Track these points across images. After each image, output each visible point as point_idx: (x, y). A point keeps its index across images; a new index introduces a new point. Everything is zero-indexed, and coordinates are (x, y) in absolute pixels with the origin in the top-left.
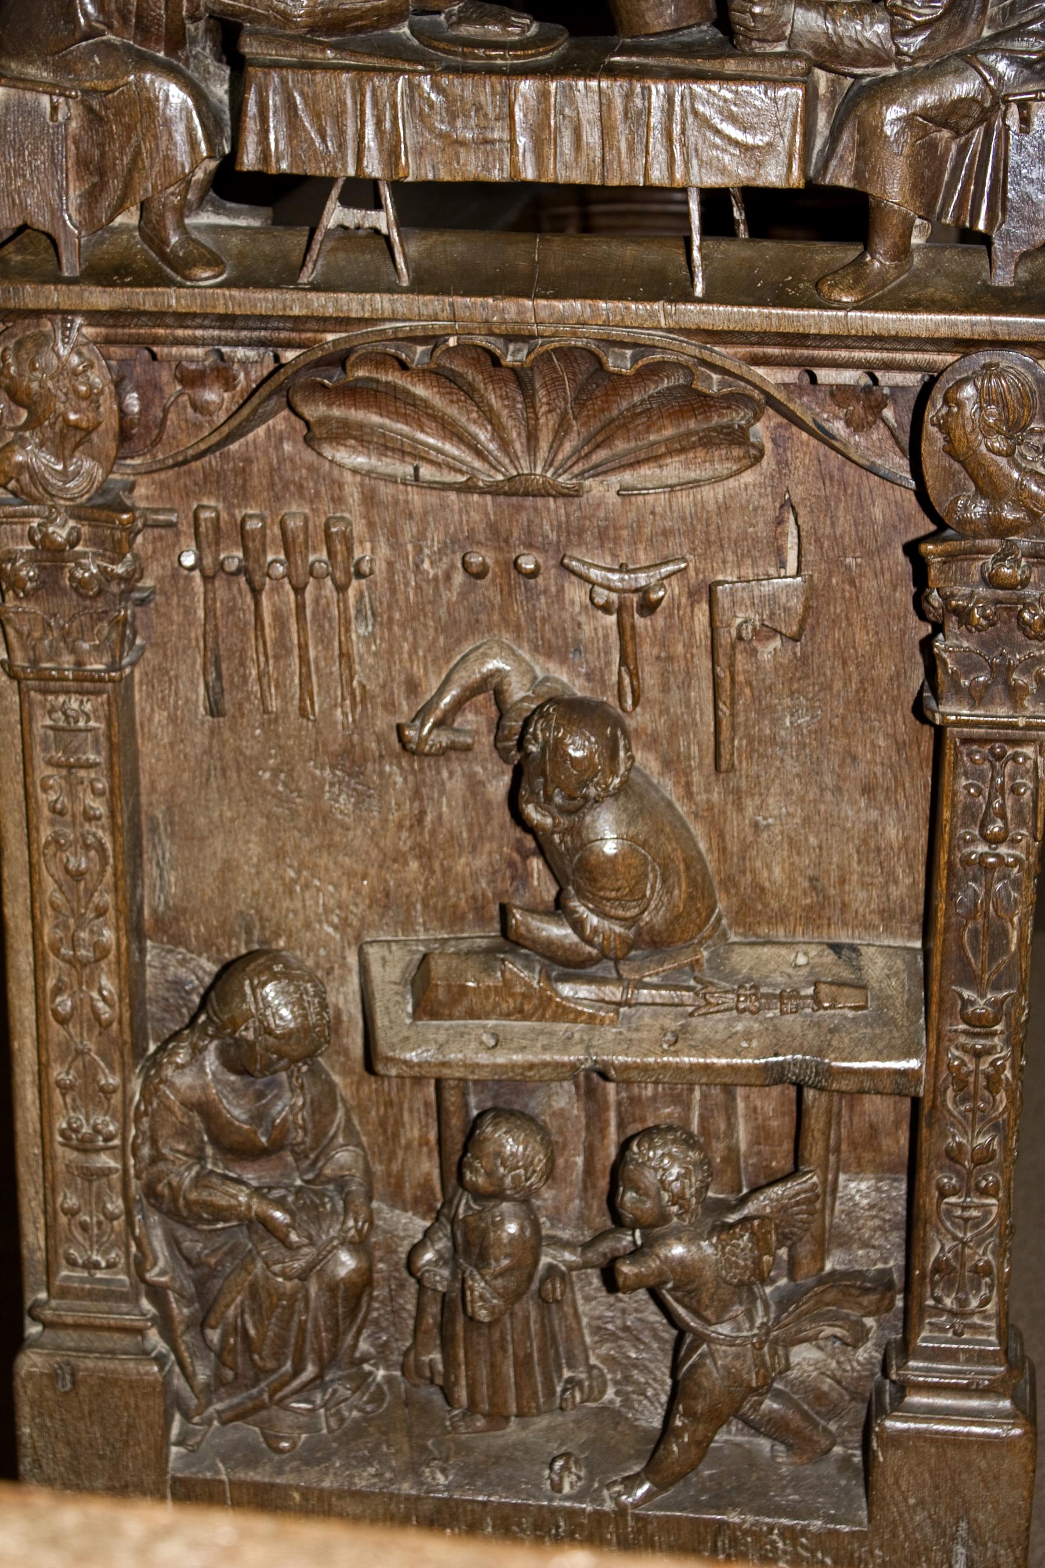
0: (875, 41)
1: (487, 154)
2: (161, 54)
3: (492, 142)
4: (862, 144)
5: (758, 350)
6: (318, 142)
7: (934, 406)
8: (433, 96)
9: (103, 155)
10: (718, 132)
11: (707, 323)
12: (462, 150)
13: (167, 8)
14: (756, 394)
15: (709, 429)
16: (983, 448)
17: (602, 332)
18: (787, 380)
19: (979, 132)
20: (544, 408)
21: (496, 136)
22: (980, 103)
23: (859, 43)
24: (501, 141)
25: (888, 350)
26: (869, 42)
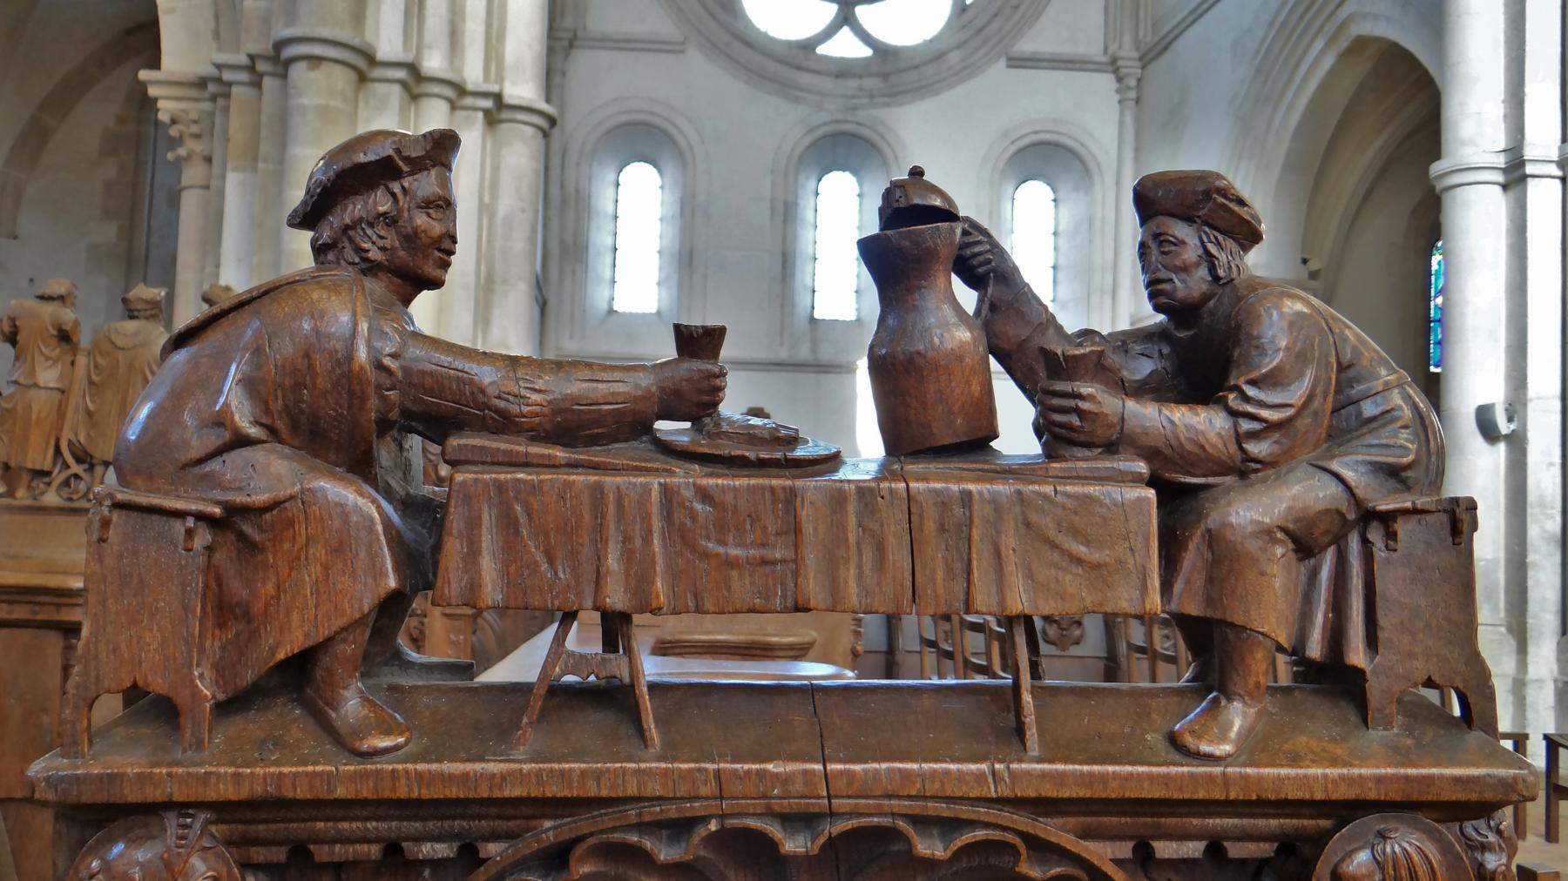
0: (1220, 445)
3: (773, 562)
5: (1092, 820)
6: (544, 567)
8: (699, 507)
10: (1054, 546)
11: (1049, 791)
12: (735, 573)
17: (916, 807)
18: (1120, 855)
21: (778, 555)
23: (1202, 447)
24: (783, 561)
25: (1286, 816)
26: (1215, 446)
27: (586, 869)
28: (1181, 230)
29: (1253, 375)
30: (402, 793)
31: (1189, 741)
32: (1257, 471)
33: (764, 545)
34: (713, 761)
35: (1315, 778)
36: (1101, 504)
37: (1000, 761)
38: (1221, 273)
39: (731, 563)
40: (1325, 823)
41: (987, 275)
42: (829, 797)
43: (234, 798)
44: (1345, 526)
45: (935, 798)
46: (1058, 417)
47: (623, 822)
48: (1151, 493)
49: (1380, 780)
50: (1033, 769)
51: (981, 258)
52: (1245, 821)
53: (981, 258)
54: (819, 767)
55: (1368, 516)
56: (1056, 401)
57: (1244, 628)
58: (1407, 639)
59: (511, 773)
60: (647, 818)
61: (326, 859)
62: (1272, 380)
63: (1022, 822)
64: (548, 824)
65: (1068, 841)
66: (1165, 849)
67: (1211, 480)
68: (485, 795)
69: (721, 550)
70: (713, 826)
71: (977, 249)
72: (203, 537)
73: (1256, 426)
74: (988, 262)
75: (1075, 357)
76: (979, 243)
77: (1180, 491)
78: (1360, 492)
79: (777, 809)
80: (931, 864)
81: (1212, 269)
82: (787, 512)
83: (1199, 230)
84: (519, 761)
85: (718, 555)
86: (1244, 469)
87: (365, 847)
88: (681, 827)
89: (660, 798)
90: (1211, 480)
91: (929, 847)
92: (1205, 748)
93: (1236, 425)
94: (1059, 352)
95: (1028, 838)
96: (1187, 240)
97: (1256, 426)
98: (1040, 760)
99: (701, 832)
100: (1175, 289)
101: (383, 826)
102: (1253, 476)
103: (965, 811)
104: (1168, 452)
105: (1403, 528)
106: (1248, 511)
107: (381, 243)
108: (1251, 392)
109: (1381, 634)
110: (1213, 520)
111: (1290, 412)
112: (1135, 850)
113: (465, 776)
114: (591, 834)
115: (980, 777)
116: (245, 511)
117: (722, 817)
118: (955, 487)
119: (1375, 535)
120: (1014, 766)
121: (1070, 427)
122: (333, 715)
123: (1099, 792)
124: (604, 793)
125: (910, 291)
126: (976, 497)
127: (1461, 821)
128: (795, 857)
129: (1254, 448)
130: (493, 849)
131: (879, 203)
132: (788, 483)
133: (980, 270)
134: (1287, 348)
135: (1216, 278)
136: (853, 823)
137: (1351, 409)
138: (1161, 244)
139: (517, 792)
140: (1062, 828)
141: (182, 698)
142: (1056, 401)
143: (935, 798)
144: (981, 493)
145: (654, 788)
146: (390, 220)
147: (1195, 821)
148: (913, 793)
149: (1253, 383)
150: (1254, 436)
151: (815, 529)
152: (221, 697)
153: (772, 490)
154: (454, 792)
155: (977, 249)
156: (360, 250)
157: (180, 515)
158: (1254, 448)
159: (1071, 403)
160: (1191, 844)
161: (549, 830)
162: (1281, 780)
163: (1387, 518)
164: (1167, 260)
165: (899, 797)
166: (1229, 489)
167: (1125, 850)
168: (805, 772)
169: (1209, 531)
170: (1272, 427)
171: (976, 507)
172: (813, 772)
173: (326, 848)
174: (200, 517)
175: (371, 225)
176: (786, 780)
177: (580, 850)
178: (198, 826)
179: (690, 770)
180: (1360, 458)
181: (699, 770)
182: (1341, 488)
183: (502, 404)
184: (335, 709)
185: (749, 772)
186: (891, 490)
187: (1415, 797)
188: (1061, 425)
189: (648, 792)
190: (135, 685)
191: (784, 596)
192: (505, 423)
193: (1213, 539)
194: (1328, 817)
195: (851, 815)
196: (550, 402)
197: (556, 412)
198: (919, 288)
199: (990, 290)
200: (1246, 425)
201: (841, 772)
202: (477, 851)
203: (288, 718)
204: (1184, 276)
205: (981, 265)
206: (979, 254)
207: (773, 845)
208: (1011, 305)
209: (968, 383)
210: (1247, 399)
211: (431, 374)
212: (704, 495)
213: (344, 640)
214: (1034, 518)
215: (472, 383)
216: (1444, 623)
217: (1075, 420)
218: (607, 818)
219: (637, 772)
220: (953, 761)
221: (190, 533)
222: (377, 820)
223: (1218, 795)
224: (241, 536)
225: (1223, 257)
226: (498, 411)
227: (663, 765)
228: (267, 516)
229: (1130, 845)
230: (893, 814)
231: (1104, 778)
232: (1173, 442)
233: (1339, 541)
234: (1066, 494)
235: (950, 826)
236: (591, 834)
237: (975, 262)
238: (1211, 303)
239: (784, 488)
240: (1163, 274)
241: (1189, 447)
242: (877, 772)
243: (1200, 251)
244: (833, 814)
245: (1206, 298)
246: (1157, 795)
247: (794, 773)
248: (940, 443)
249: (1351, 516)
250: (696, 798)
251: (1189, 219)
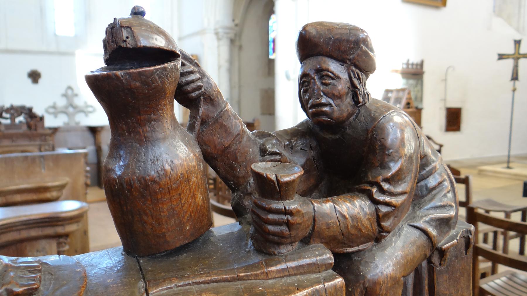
23: (360, 230)
28: (334, 67)
41: (198, 98)
51: (194, 85)
53: (194, 85)
56: (271, 217)
67: (361, 247)
74: (200, 88)
76: (191, 72)
83: (348, 69)
90: (361, 247)
93: (377, 210)
96: (341, 75)
100: (333, 111)
104: (340, 237)
108: (386, 186)
125: (141, 124)
131: (103, 36)
133: (193, 95)
137: (422, 183)
138: (321, 78)
149: (387, 180)
164: (328, 89)
169: (366, 288)
198: (149, 121)
199: (201, 110)
200: (384, 209)
204: (338, 102)
205: (194, 90)
206: (192, 82)
208: (216, 121)
209: (194, 197)
210: (382, 191)
232: (344, 231)
237: (189, 88)
241: (353, 231)
243: (349, 84)
248: (173, 247)
251: (342, 61)
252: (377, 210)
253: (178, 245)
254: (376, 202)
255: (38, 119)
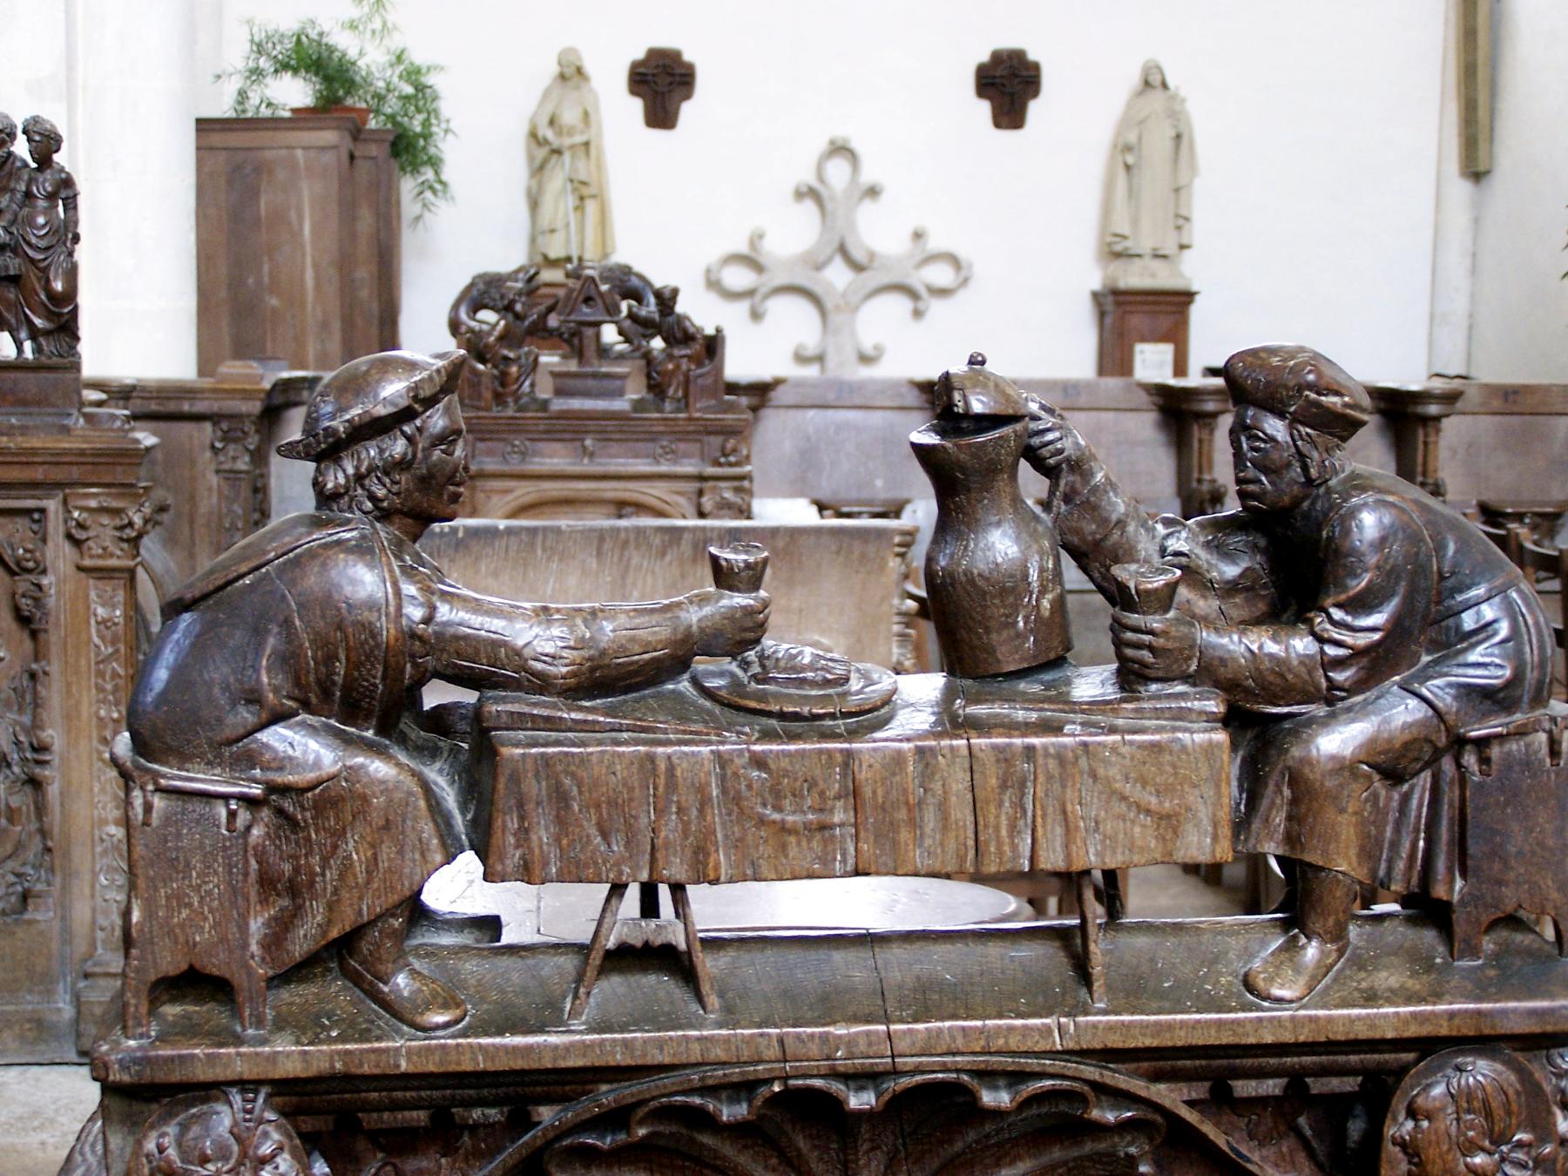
1: (825, 842)
2: (370, 734)
3: (831, 827)
4: (1294, 801)
7: (1395, 1119)
9: (297, 870)
10: (1124, 798)
11: (1115, 1041)
12: (792, 839)
13: (384, 678)
14: (1159, 1119)
15: (1080, 1158)
16: (1462, 1167)
18: (1194, 1095)
19: (1425, 778)
20: (866, 1146)
21: (836, 819)
22: (1428, 740)
23: (1283, 676)
24: (842, 825)
27: (642, 1132)
29: (1343, 597)
30: (467, 1066)
31: (1260, 983)
32: (1343, 699)
33: (821, 810)
34: (776, 1027)
35: (1386, 1016)
36: (1171, 753)
37: (1067, 1015)
38: (1313, 472)
39: (783, 829)
40: (1411, 1056)
42: (893, 1057)
43: (303, 1075)
44: (1437, 754)
45: (999, 1053)
46: (1129, 652)
47: (686, 1086)
48: (1221, 736)
49: (1452, 1015)
50: (1104, 1022)
52: (1324, 1058)
54: (884, 1027)
55: (1459, 743)
56: (1129, 635)
57: (1322, 869)
58: (1497, 866)
59: (572, 1044)
60: (710, 1082)
61: (373, 1126)
62: (1362, 604)
63: (1091, 1072)
64: (604, 1088)
65: (1138, 1086)
66: (1245, 1088)
67: (1295, 709)
68: (549, 1066)
69: (776, 816)
70: (777, 1088)
71: (1050, 437)
72: (243, 816)
73: (1341, 652)
75: (1148, 592)
76: (1049, 430)
77: (1258, 721)
78: (1451, 719)
79: (842, 1069)
80: (997, 1114)
81: (1305, 468)
82: (844, 775)
84: (581, 1032)
85: (774, 822)
86: (1330, 696)
87: (415, 1114)
88: (744, 1089)
89: (724, 1063)
90: (1295, 709)
91: (996, 1098)
92: (1277, 992)
94: (1132, 585)
95: (1094, 1085)
97: (1341, 652)
98: (1105, 1012)
99: (763, 1092)
101: (436, 1094)
102: (1340, 705)
103: (1033, 1063)
105: (1495, 752)
106: (1338, 740)
107: (395, 488)
109: (1470, 863)
110: (1296, 752)
111: (1377, 636)
112: (1212, 1090)
113: (529, 1049)
114: (653, 1098)
115: (1047, 1031)
116: (285, 790)
117: (785, 1079)
118: (1018, 741)
119: (1470, 759)
120: (1080, 1019)
121: (1144, 665)
122: (386, 989)
123: (1166, 1041)
124: (667, 1060)
126: (1040, 752)
127: (1548, 1048)
128: (859, 1114)
129: (1340, 676)
130: (546, 1114)
132: (846, 746)
133: (1052, 461)
134: (1378, 567)
135: (1309, 481)
136: (919, 1078)
137: (1451, 621)
139: (580, 1063)
140: (1130, 1074)
141: (239, 979)
142: (1129, 635)
143: (999, 1053)
144: (1045, 747)
145: (718, 1053)
146: (403, 464)
147: (1272, 1061)
148: (978, 1049)
149: (1339, 606)
150: (1339, 663)
151: (874, 792)
152: (271, 973)
153: (829, 752)
154: (519, 1064)
155: (1050, 437)
156: (372, 497)
157: (226, 797)
158: (1340, 676)
159: (1147, 638)
160: (1271, 1082)
161: (607, 1095)
162: (1351, 1020)
163: (1482, 743)
165: (962, 1054)
166: (1311, 721)
167: (1199, 1091)
168: (868, 1033)
170: (1358, 653)
171: (1041, 761)
172: (877, 1032)
173: (375, 1115)
174: (245, 799)
175: (387, 474)
176: (851, 1041)
177: (641, 1112)
178: (261, 1100)
179: (752, 1035)
180: (1453, 679)
181: (762, 1035)
182: (1430, 712)
183: (539, 666)
184: (386, 983)
185: (812, 1035)
186: (952, 748)
187: (1486, 1031)
188: (1134, 661)
189: (712, 1057)
190: (191, 968)
191: (844, 861)
192: (542, 684)
193: (1294, 778)
194: (1410, 1051)
195: (918, 1070)
196: (590, 659)
197: (592, 670)
199: (1062, 483)
200: (1331, 651)
201: (904, 1032)
202: (529, 1115)
203: (336, 992)
204: (1273, 476)
207: (837, 1103)
211: (466, 637)
212: (759, 762)
213: (393, 916)
214: (1101, 772)
215: (505, 644)
216: (1539, 851)
217: (1146, 655)
218: (668, 1081)
219: (699, 1039)
220: (1019, 1016)
221: (232, 815)
222: (430, 1089)
223: (1287, 1037)
224: (280, 812)
225: (1315, 455)
226: (535, 674)
227: (724, 1032)
228: (310, 795)
229: (1207, 1084)
230: (957, 1071)
231: (1170, 1026)
233: (1433, 762)
234: (1131, 743)
235: (1016, 1078)
236: (653, 1098)
238: (1306, 505)
239: (841, 751)
240: (1251, 472)
241: (1271, 678)
242: (940, 1030)
244: (896, 1073)
245: (1297, 502)
246: (1224, 1041)
247: (857, 1034)
249: (1442, 741)
250: (761, 1062)
251: (1281, 415)
252: (1322, 651)
253: (1012, 668)
254: (1321, 640)
255: (697, 347)
